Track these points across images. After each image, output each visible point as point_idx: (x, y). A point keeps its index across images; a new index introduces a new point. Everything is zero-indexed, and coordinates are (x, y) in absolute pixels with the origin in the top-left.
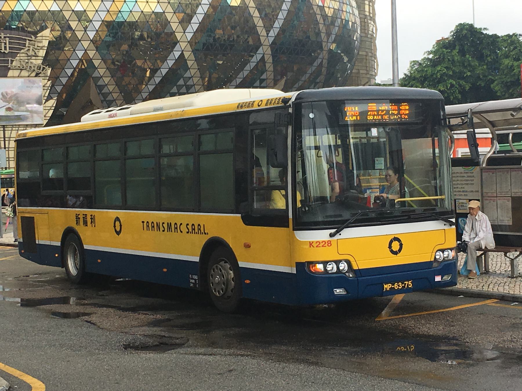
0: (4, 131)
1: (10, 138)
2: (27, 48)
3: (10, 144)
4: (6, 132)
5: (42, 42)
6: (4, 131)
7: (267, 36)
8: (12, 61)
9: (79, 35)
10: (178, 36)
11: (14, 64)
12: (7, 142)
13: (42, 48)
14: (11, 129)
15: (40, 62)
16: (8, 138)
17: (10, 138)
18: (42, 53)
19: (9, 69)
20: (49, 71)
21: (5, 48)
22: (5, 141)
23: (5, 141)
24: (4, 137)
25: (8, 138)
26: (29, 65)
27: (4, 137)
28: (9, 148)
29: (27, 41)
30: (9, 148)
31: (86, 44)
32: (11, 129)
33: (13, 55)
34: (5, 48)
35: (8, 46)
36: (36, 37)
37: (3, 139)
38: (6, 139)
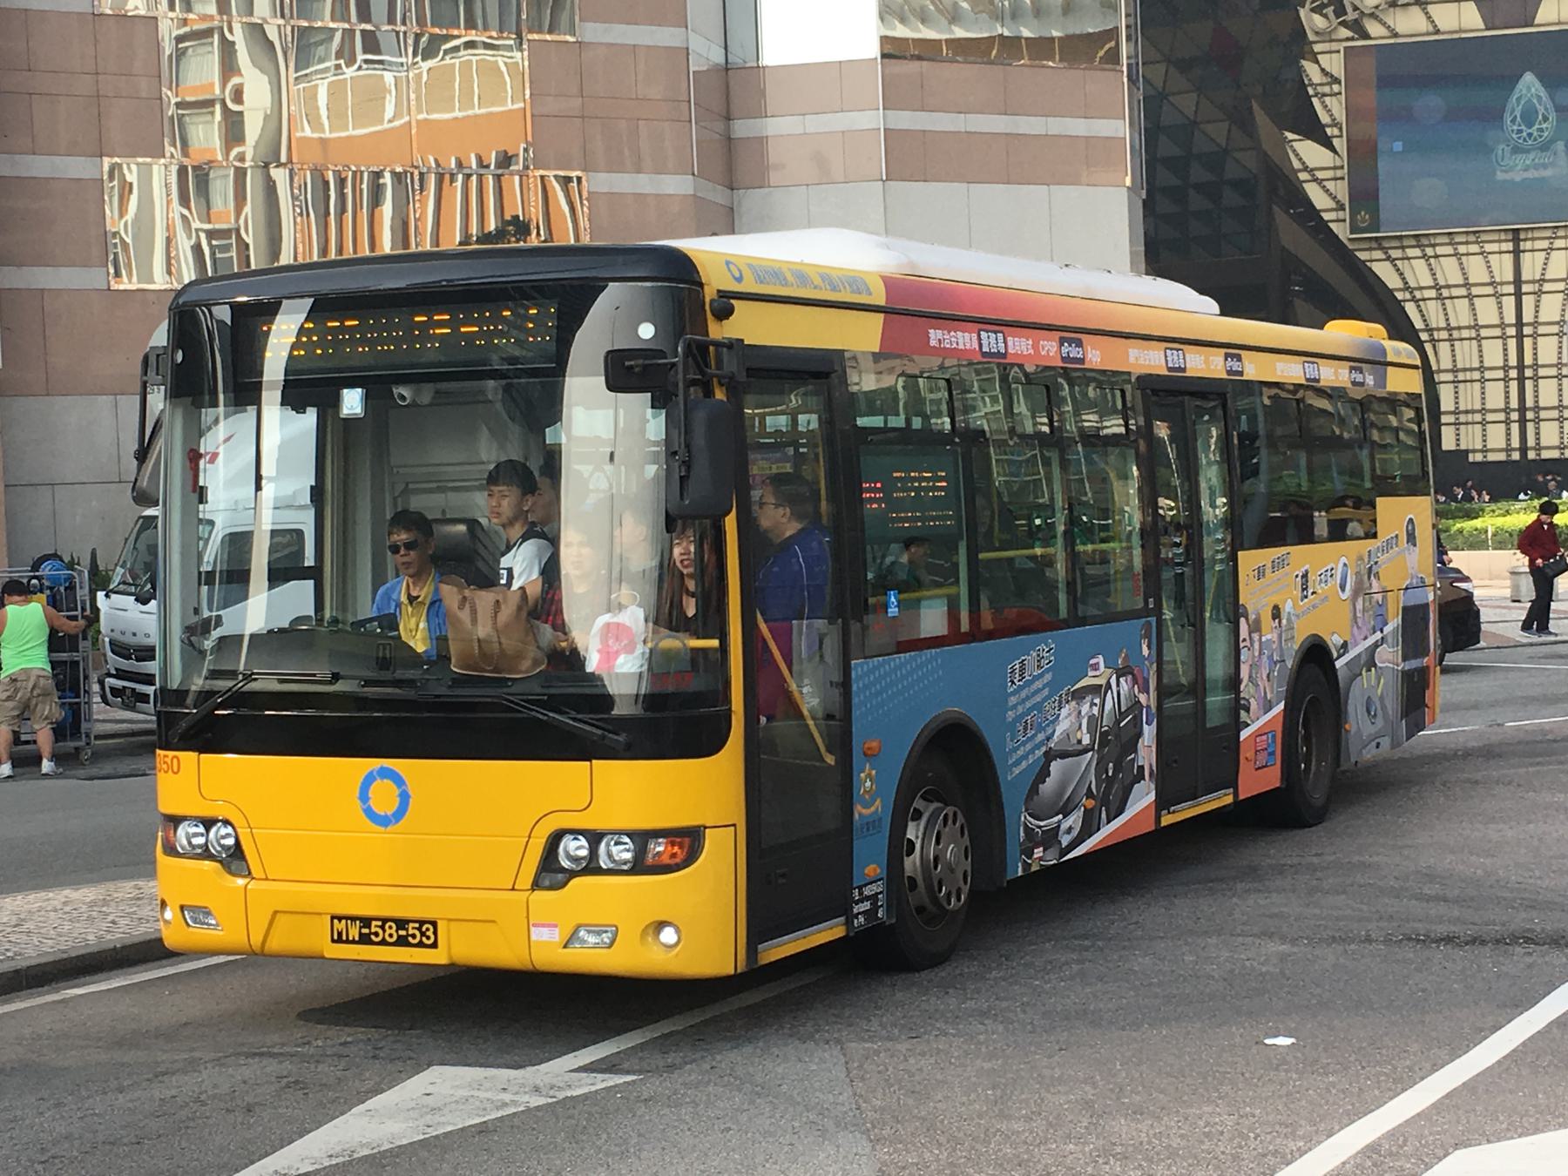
0: (1517, 253)
1: (1543, 280)
3: (1540, 314)
4: (1526, 259)
6: (1517, 253)
12: (1528, 302)
14: (1545, 244)
16: (1533, 282)
17: (1543, 280)
22: (1518, 295)
23: (1518, 295)
24: (1518, 281)
25: (1533, 282)
27: (1518, 281)
28: (1535, 324)
30: (1535, 324)
32: (1545, 244)
37: (1511, 289)
38: (1525, 288)
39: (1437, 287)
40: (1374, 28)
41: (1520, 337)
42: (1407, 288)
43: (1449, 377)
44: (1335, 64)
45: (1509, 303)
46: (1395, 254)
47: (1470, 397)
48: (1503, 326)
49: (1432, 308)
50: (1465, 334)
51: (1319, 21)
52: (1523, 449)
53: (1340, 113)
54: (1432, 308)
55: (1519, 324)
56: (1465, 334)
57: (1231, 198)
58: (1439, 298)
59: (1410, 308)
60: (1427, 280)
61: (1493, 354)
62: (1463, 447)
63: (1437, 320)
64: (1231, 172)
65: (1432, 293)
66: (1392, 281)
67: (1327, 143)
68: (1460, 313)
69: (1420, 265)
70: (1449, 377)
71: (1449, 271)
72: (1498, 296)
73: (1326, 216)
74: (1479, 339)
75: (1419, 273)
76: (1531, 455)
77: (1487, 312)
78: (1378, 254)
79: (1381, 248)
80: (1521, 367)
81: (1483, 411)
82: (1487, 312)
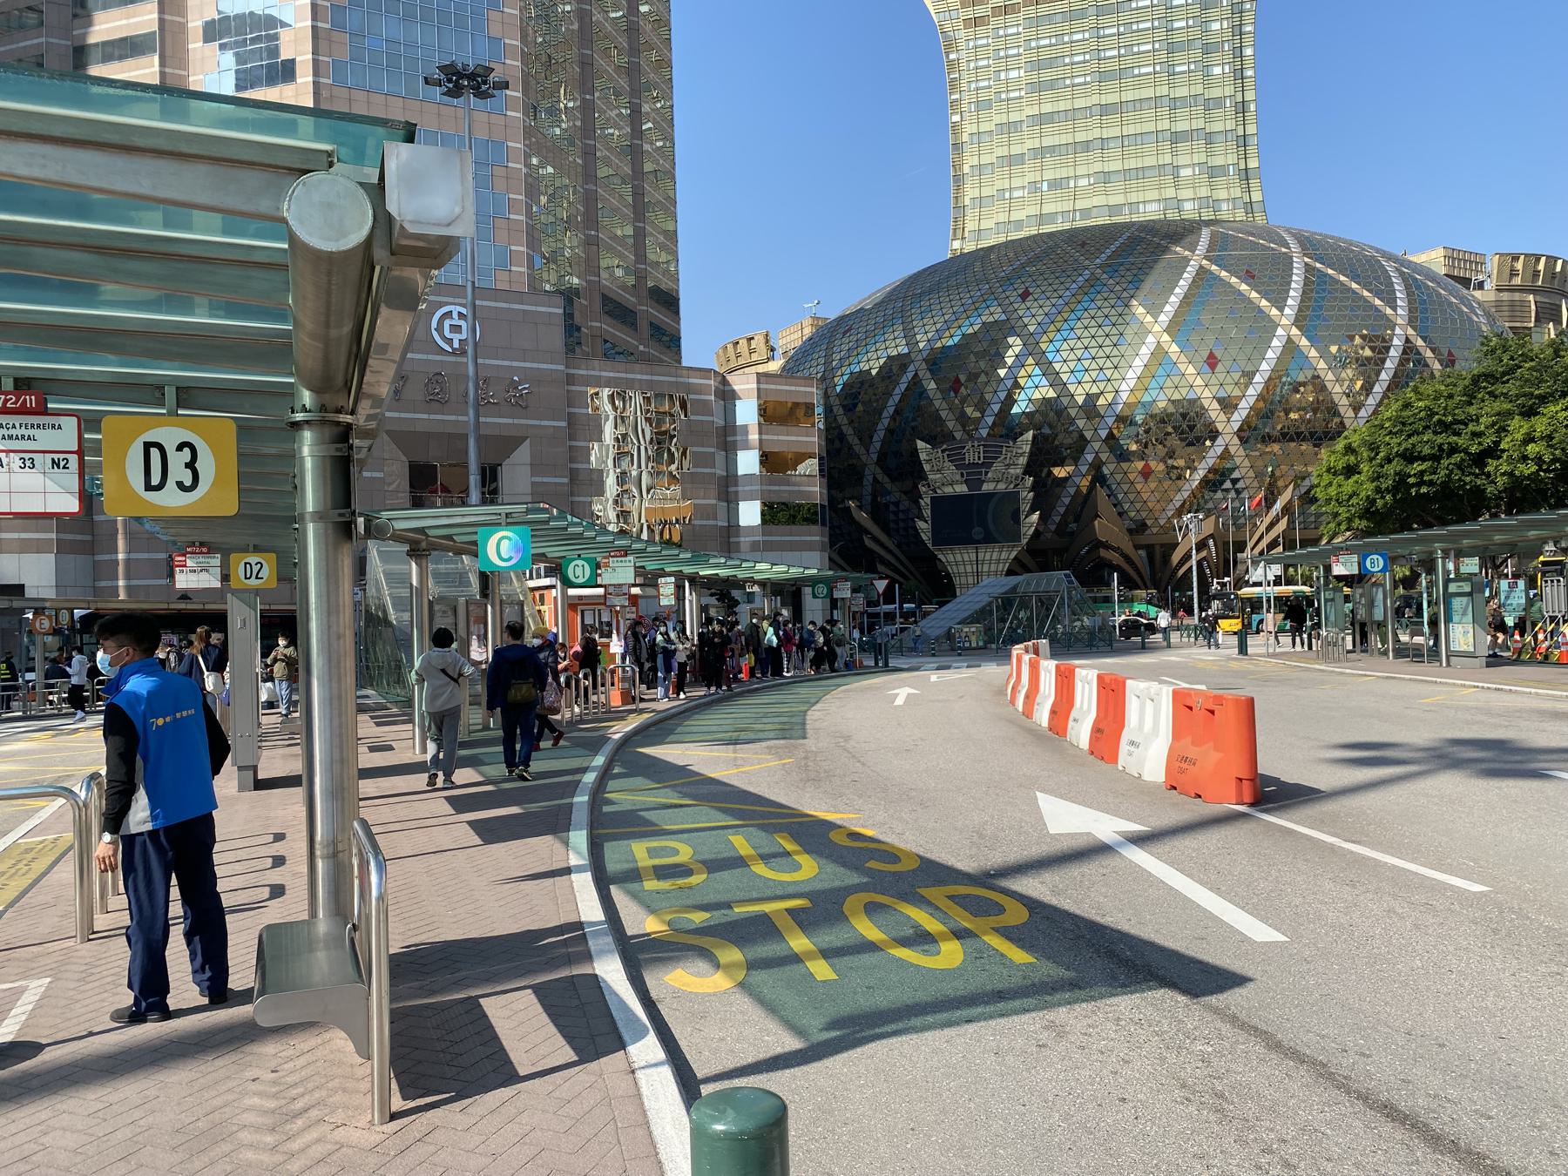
2: (1003, 457)
5: (1021, 448)
7: (1356, 417)
8: (986, 473)
9: (1088, 435)
10: (1220, 427)
11: (990, 475)
12: (980, 566)
13: (1021, 455)
15: (1019, 471)
18: (1023, 460)
19: (984, 481)
20: (1030, 481)
21: (979, 459)
26: (1005, 476)
29: (1004, 449)
31: (1096, 445)
33: (988, 465)
34: (979, 459)
35: (982, 455)
36: (1015, 442)
40: (939, 491)
44: (928, 501)
45: (975, 566)
51: (924, 489)
53: (929, 512)
57: (901, 516)
59: (949, 568)
64: (901, 507)
66: (944, 560)
67: (926, 522)
68: (962, 569)
71: (959, 557)
75: (951, 558)
77: (969, 569)
82: (969, 569)
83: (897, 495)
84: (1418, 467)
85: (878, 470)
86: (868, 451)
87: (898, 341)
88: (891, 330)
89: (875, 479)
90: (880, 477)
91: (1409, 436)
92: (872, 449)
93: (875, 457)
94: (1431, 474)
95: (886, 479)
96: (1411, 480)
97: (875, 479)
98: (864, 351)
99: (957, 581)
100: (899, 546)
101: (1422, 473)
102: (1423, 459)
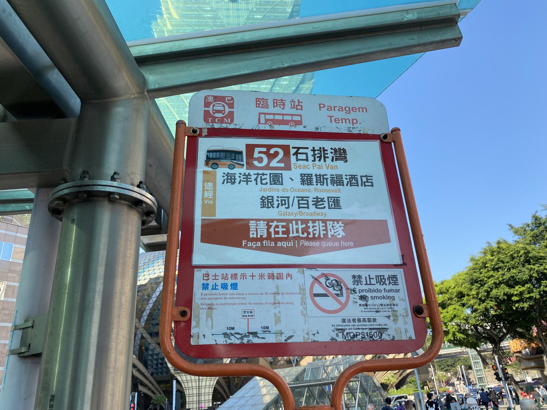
12: (200, 383)
22: (199, 381)
23: (199, 381)
28: (201, 386)
30: (201, 386)
37: (198, 380)
38: (200, 380)
39: (187, 380)
41: (199, 388)
42: (182, 381)
43: (188, 396)
45: (198, 383)
46: (181, 375)
47: (191, 399)
48: (196, 387)
49: (186, 384)
50: (191, 388)
52: (199, 408)
54: (186, 384)
55: (199, 386)
56: (191, 388)
58: (187, 382)
60: (185, 379)
61: (195, 392)
62: (190, 408)
63: (187, 386)
64: (156, 352)
65: (186, 381)
69: (184, 377)
70: (188, 396)
72: (196, 382)
73: (170, 369)
74: (193, 389)
76: (200, 409)
77: (194, 384)
78: (178, 375)
79: (178, 374)
80: (199, 394)
81: (193, 401)
82: (194, 384)
83: (154, 345)
84: (518, 289)
85: (144, 331)
86: (140, 321)
87: (160, 267)
88: (157, 262)
89: (142, 337)
90: (145, 335)
91: (509, 269)
92: (142, 320)
93: (143, 324)
94: (529, 293)
95: (148, 336)
96: (515, 298)
97: (142, 337)
98: (143, 271)
99: (187, 393)
100: (152, 374)
101: (521, 293)
102: (523, 283)
